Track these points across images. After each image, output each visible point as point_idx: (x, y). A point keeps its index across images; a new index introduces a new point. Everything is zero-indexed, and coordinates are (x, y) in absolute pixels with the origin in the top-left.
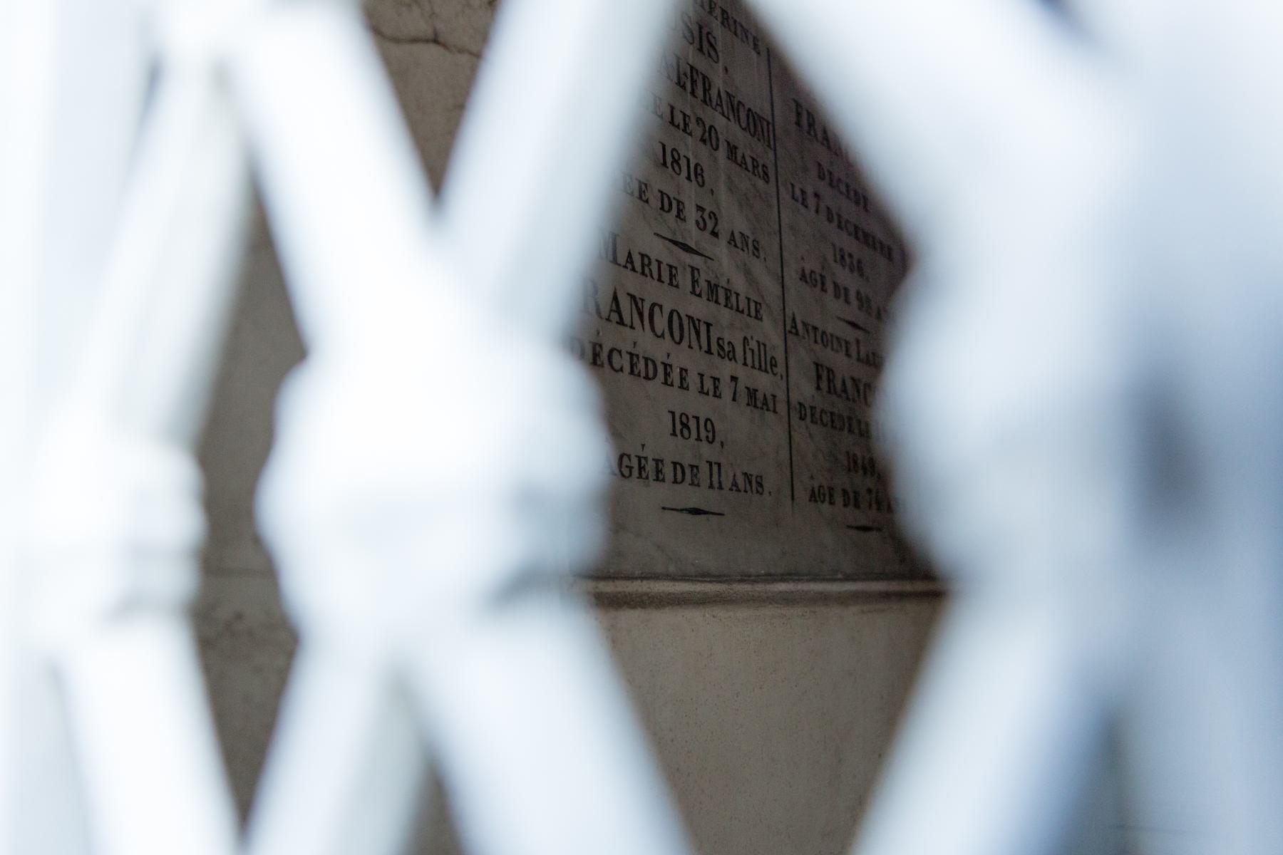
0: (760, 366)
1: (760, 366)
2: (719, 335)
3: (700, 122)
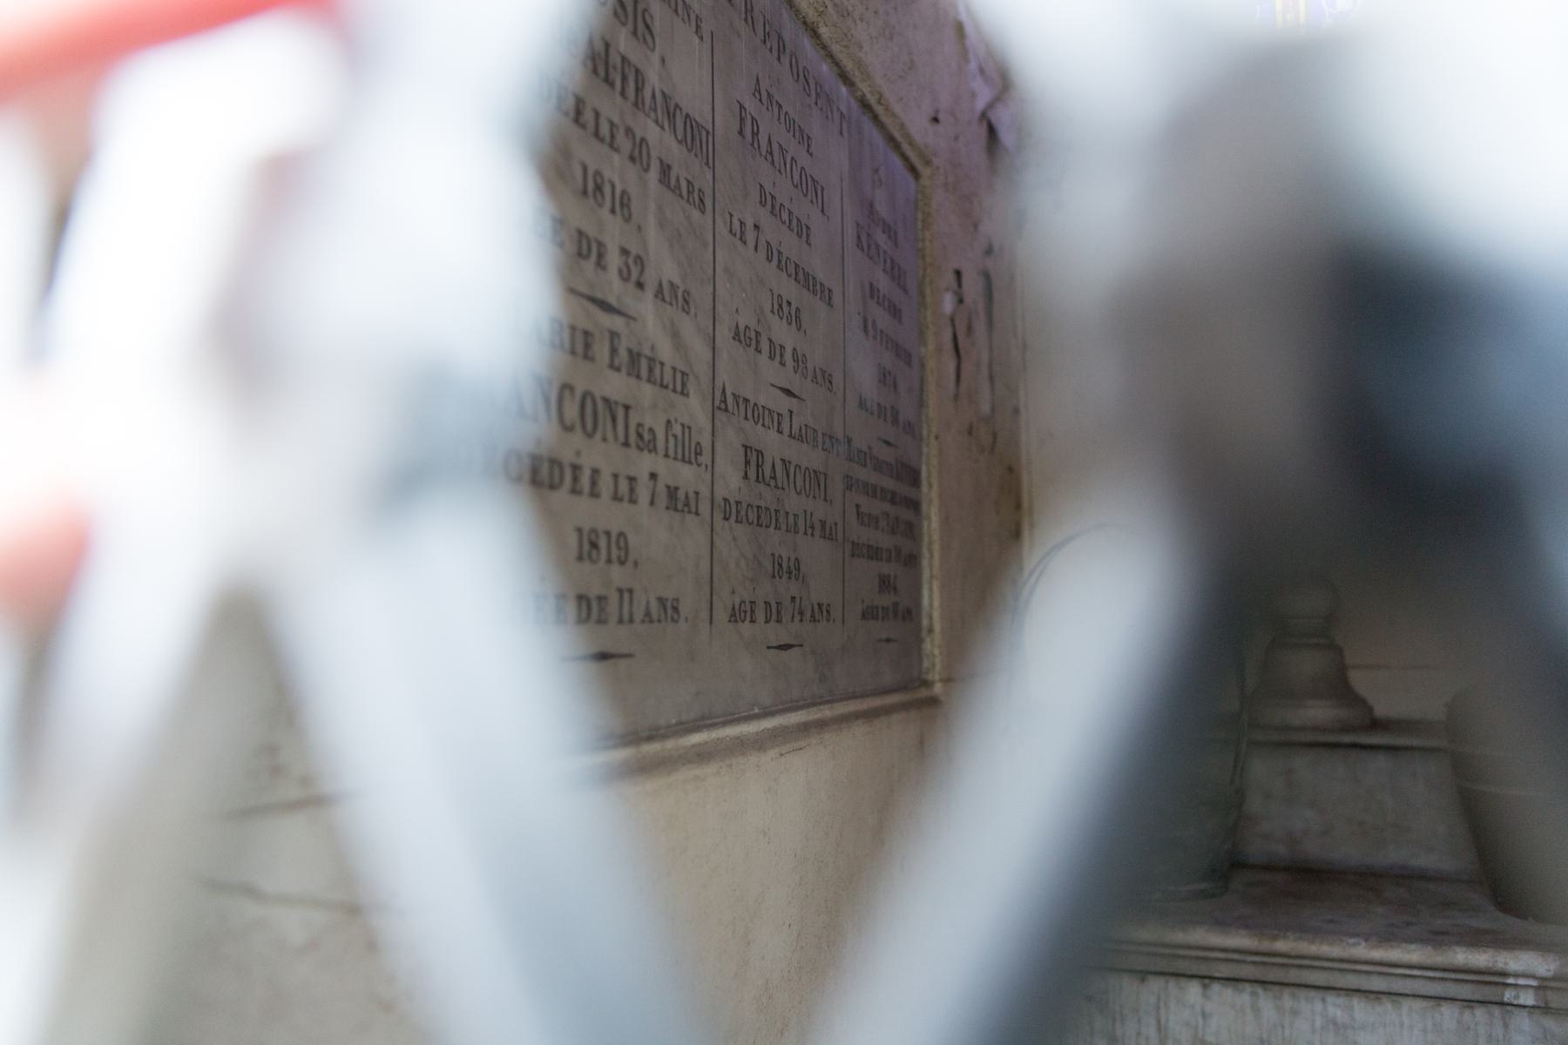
0: (831, 534)
1: (831, 534)
2: (727, 523)
3: (638, 261)
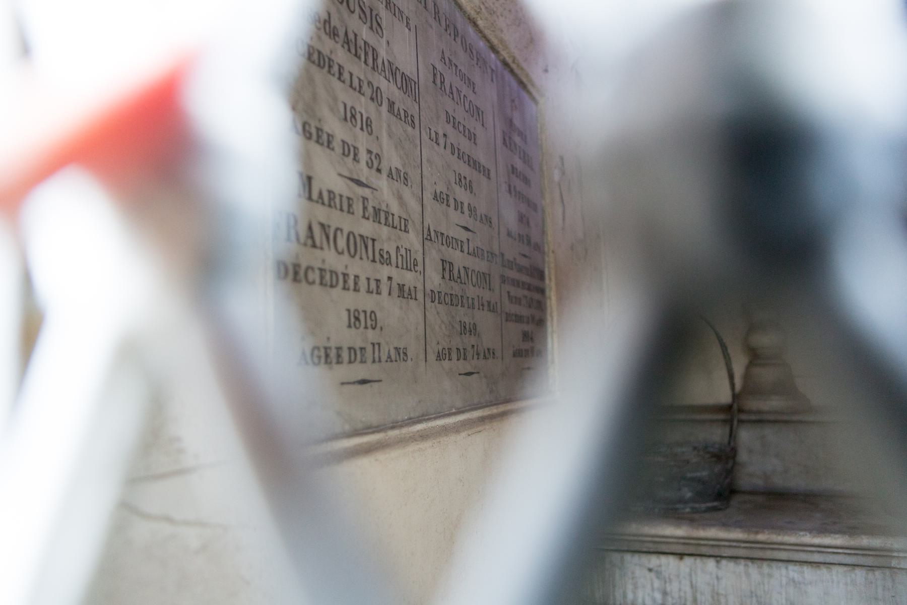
2: (433, 304)
